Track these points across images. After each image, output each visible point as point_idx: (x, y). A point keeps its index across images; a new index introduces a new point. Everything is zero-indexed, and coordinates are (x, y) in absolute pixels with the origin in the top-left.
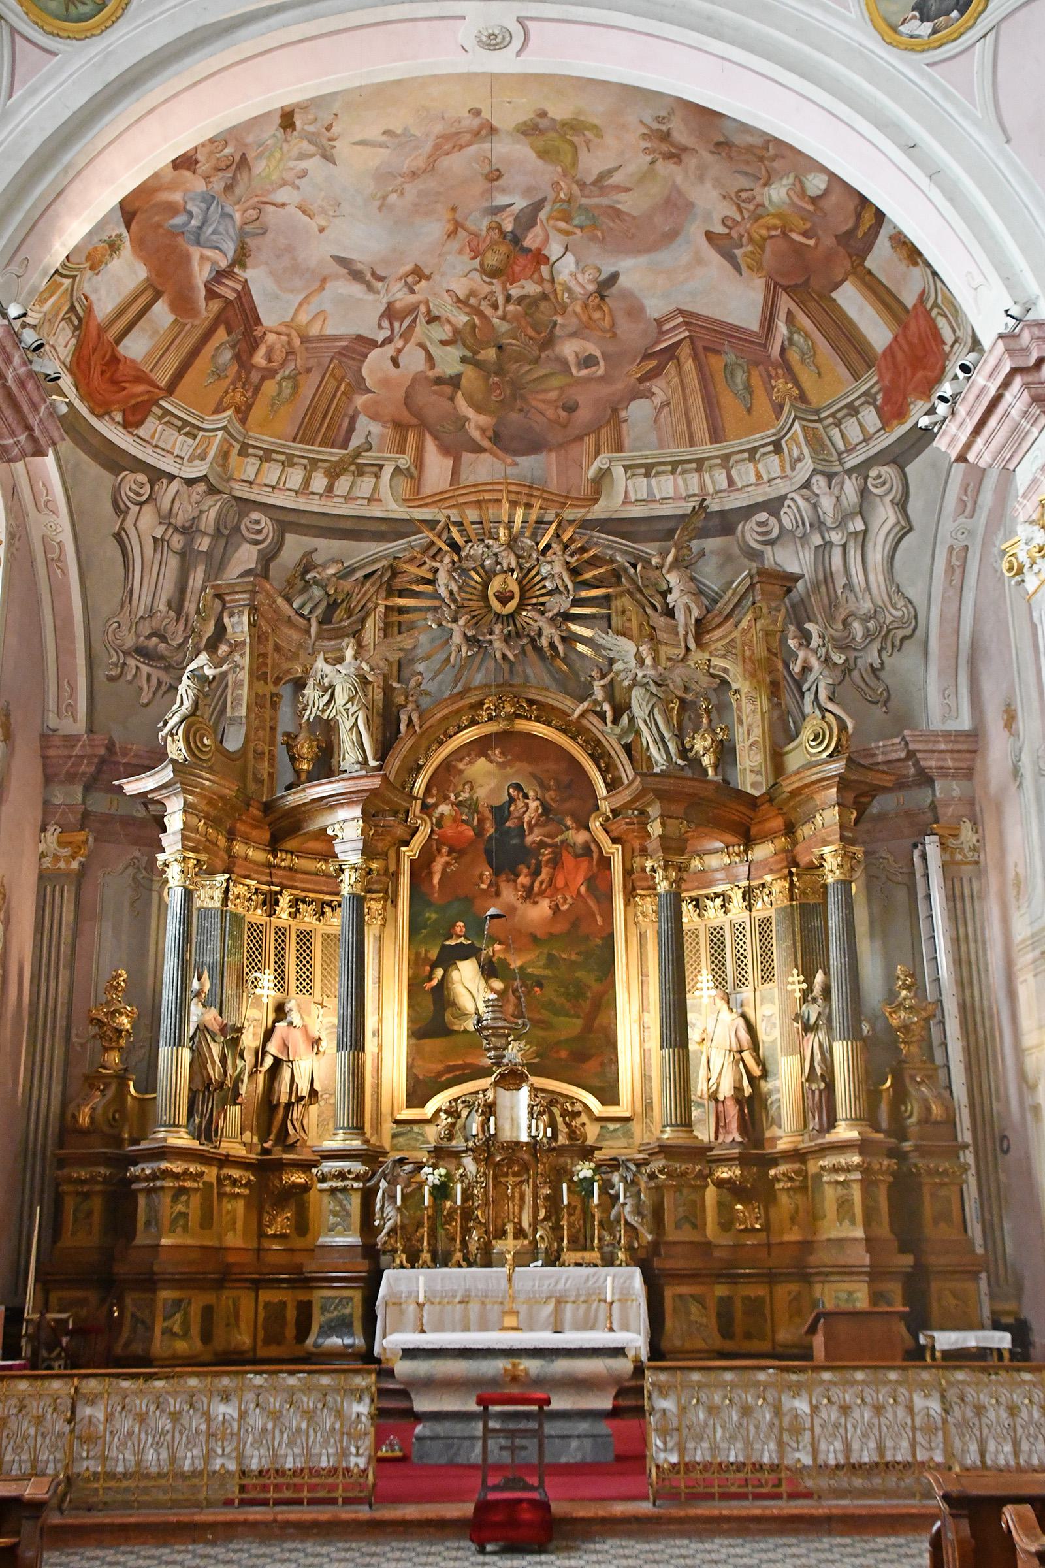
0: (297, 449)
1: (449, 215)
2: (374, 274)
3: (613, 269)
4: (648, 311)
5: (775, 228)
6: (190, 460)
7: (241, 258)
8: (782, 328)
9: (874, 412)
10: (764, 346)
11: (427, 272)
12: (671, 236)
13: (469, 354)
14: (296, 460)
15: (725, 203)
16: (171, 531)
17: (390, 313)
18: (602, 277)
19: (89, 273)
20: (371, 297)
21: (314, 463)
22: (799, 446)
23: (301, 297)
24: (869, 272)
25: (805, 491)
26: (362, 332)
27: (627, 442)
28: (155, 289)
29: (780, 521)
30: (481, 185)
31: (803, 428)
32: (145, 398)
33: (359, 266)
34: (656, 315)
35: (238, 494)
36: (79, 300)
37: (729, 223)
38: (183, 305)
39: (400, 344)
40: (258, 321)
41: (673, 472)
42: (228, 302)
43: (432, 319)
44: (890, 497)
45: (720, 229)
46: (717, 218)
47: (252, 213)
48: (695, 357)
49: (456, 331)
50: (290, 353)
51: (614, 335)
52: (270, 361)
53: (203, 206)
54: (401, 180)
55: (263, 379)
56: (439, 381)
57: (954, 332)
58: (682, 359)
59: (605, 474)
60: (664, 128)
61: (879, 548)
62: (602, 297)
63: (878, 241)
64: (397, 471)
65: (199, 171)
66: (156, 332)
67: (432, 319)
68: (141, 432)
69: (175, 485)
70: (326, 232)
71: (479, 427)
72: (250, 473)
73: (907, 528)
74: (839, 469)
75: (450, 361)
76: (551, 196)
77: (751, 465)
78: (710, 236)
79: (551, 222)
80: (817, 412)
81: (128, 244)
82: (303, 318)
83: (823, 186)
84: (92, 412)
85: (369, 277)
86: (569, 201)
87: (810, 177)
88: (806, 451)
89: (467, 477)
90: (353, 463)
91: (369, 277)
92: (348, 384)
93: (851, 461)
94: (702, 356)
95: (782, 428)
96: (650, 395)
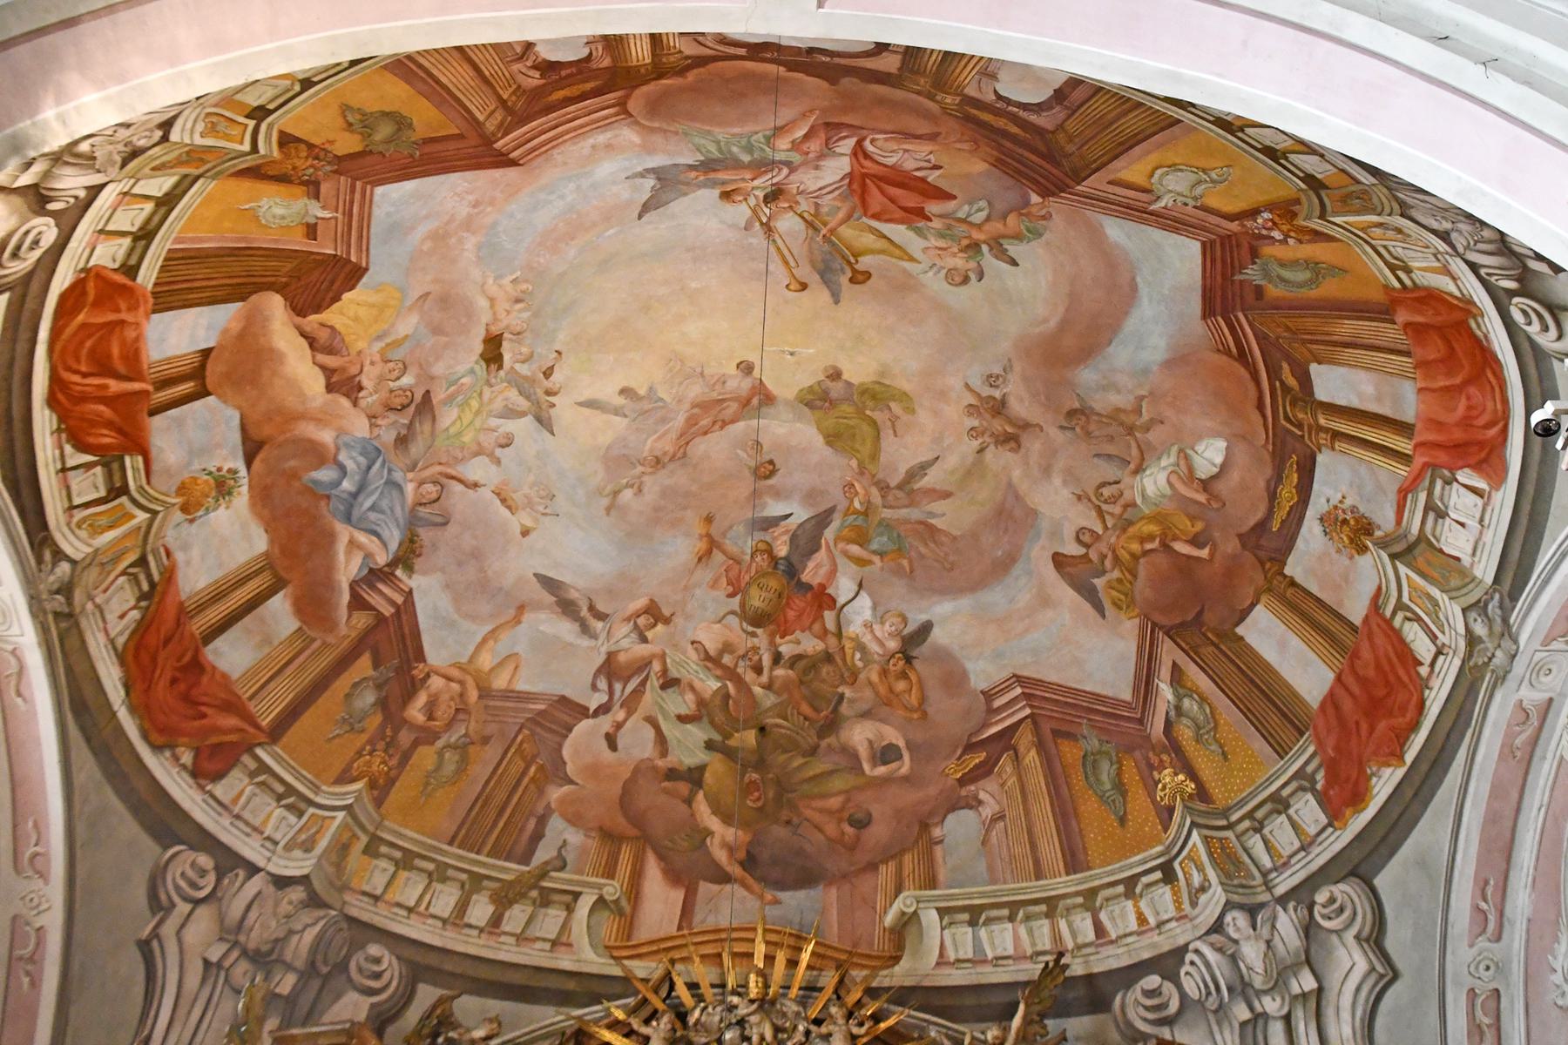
0: (454, 855)
1: (699, 529)
2: (591, 608)
3: (924, 617)
4: (972, 678)
5: (1151, 538)
6: (288, 847)
7: (407, 556)
8: (1166, 692)
9: (1313, 802)
10: (1141, 721)
11: (666, 612)
12: (1003, 566)
13: (717, 737)
14: (450, 872)
15: (1080, 507)
16: (235, 954)
17: (610, 669)
19: (178, 516)
20: (586, 642)
21: (476, 881)
22: (1200, 869)
23: (489, 628)
24: (1293, 583)
25: (1215, 938)
26: (568, 693)
27: (942, 874)
28: (275, 574)
29: (1179, 986)
30: (745, 485)
31: (1206, 840)
32: (233, 738)
33: (573, 595)
34: (984, 686)
35: (354, 912)
36: (155, 552)
37: (1086, 538)
38: (312, 608)
39: (621, 715)
40: (420, 655)
41: (1011, 919)
42: (381, 619)
43: (669, 683)
44: (1354, 930)
45: (1073, 549)
46: (1069, 532)
47: (431, 490)
48: (1041, 746)
50: (462, 710)
51: (925, 715)
52: (431, 718)
53: (362, 460)
54: (640, 469)
55: (416, 744)
56: (672, 774)
57: (1434, 638)
58: (1022, 749)
59: (909, 921)
60: (997, 394)
61: (1346, 1015)
62: (909, 660)
63: (1304, 530)
64: (601, 902)
65: (363, 403)
66: (267, 640)
67: (669, 683)
68: (219, 789)
69: (256, 883)
70: (533, 536)
71: (725, 845)
72: (377, 883)
73: (1387, 975)
74: (1266, 897)
75: (689, 746)
76: (842, 505)
77: (1130, 904)
78: (1059, 561)
79: (841, 545)
80: (1225, 813)
81: (245, 489)
82: (486, 661)
83: (1219, 460)
84: (145, 736)
85: (584, 612)
86: (866, 514)
87: (1200, 448)
88: (1212, 874)
89: (705, 918)
90: (534, 886)
91: (584, 612)
92: (541, 768)
93: (1284, 884)
94: (1050, 745)
95: (1173, 843)
96: (974, 803)
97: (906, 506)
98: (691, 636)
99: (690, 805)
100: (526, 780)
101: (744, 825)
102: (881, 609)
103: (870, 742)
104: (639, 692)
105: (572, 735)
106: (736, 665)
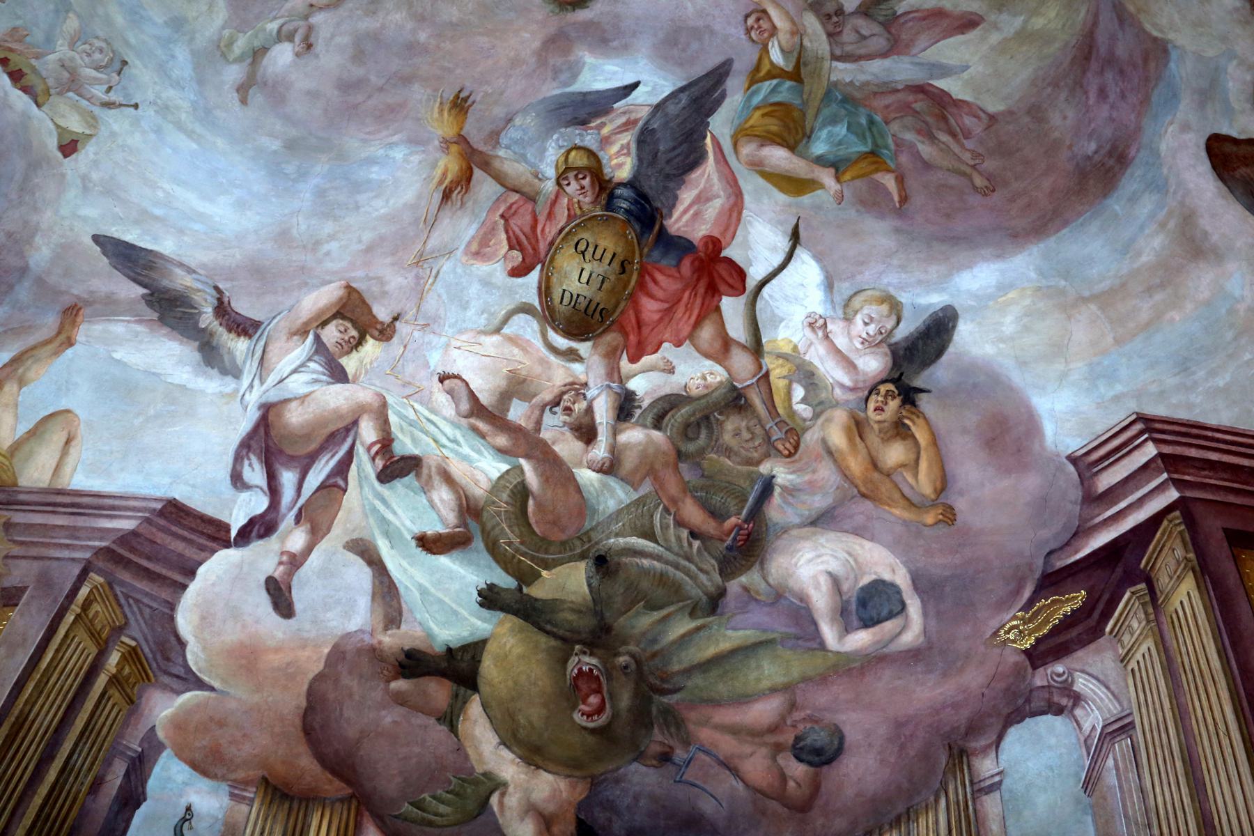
1: (441, 127)
2: (222, 309)
3: (935, 300)
4: (1049, 429)
11: (382, 313)
13: (505, 581)
18: (904, 331)
20: (211, 385)
26: (180, 493)
33: (181, 281)
34: (1074, 443)
39: (297, 540)
48: (1205, 571)
49: (469, 509)
51: (949, 515)
58: (1163, 581)
62: (909, 396)
71: (531, 809)
76: (745, 59)
79: (747, 149)
85: (207, 318)
86: (796, 75)
91: (207, 318)
92: (133, 655)
94: (1227, 566)
97: (884, 55)
98: (436, 361)
99: (453, 728)
100: (101, 681)
101: (569, 766)
102: (844, 288)
103: (835, 581)
104: (335, 486)
105: (194, 587)
106: (539, 423)
